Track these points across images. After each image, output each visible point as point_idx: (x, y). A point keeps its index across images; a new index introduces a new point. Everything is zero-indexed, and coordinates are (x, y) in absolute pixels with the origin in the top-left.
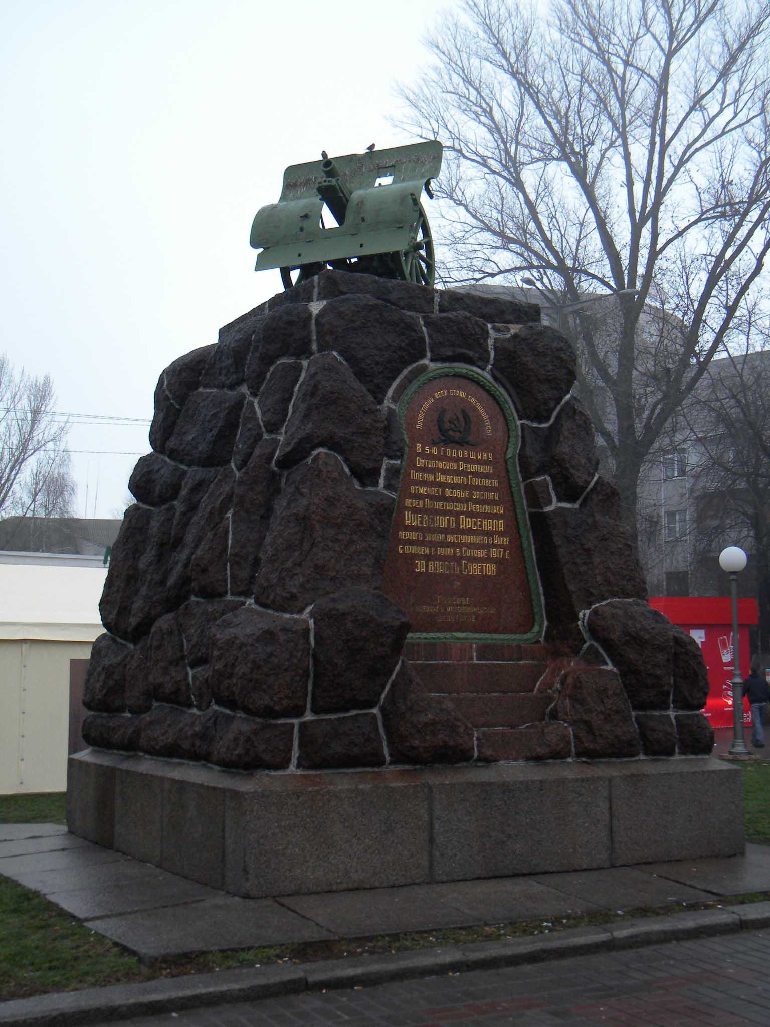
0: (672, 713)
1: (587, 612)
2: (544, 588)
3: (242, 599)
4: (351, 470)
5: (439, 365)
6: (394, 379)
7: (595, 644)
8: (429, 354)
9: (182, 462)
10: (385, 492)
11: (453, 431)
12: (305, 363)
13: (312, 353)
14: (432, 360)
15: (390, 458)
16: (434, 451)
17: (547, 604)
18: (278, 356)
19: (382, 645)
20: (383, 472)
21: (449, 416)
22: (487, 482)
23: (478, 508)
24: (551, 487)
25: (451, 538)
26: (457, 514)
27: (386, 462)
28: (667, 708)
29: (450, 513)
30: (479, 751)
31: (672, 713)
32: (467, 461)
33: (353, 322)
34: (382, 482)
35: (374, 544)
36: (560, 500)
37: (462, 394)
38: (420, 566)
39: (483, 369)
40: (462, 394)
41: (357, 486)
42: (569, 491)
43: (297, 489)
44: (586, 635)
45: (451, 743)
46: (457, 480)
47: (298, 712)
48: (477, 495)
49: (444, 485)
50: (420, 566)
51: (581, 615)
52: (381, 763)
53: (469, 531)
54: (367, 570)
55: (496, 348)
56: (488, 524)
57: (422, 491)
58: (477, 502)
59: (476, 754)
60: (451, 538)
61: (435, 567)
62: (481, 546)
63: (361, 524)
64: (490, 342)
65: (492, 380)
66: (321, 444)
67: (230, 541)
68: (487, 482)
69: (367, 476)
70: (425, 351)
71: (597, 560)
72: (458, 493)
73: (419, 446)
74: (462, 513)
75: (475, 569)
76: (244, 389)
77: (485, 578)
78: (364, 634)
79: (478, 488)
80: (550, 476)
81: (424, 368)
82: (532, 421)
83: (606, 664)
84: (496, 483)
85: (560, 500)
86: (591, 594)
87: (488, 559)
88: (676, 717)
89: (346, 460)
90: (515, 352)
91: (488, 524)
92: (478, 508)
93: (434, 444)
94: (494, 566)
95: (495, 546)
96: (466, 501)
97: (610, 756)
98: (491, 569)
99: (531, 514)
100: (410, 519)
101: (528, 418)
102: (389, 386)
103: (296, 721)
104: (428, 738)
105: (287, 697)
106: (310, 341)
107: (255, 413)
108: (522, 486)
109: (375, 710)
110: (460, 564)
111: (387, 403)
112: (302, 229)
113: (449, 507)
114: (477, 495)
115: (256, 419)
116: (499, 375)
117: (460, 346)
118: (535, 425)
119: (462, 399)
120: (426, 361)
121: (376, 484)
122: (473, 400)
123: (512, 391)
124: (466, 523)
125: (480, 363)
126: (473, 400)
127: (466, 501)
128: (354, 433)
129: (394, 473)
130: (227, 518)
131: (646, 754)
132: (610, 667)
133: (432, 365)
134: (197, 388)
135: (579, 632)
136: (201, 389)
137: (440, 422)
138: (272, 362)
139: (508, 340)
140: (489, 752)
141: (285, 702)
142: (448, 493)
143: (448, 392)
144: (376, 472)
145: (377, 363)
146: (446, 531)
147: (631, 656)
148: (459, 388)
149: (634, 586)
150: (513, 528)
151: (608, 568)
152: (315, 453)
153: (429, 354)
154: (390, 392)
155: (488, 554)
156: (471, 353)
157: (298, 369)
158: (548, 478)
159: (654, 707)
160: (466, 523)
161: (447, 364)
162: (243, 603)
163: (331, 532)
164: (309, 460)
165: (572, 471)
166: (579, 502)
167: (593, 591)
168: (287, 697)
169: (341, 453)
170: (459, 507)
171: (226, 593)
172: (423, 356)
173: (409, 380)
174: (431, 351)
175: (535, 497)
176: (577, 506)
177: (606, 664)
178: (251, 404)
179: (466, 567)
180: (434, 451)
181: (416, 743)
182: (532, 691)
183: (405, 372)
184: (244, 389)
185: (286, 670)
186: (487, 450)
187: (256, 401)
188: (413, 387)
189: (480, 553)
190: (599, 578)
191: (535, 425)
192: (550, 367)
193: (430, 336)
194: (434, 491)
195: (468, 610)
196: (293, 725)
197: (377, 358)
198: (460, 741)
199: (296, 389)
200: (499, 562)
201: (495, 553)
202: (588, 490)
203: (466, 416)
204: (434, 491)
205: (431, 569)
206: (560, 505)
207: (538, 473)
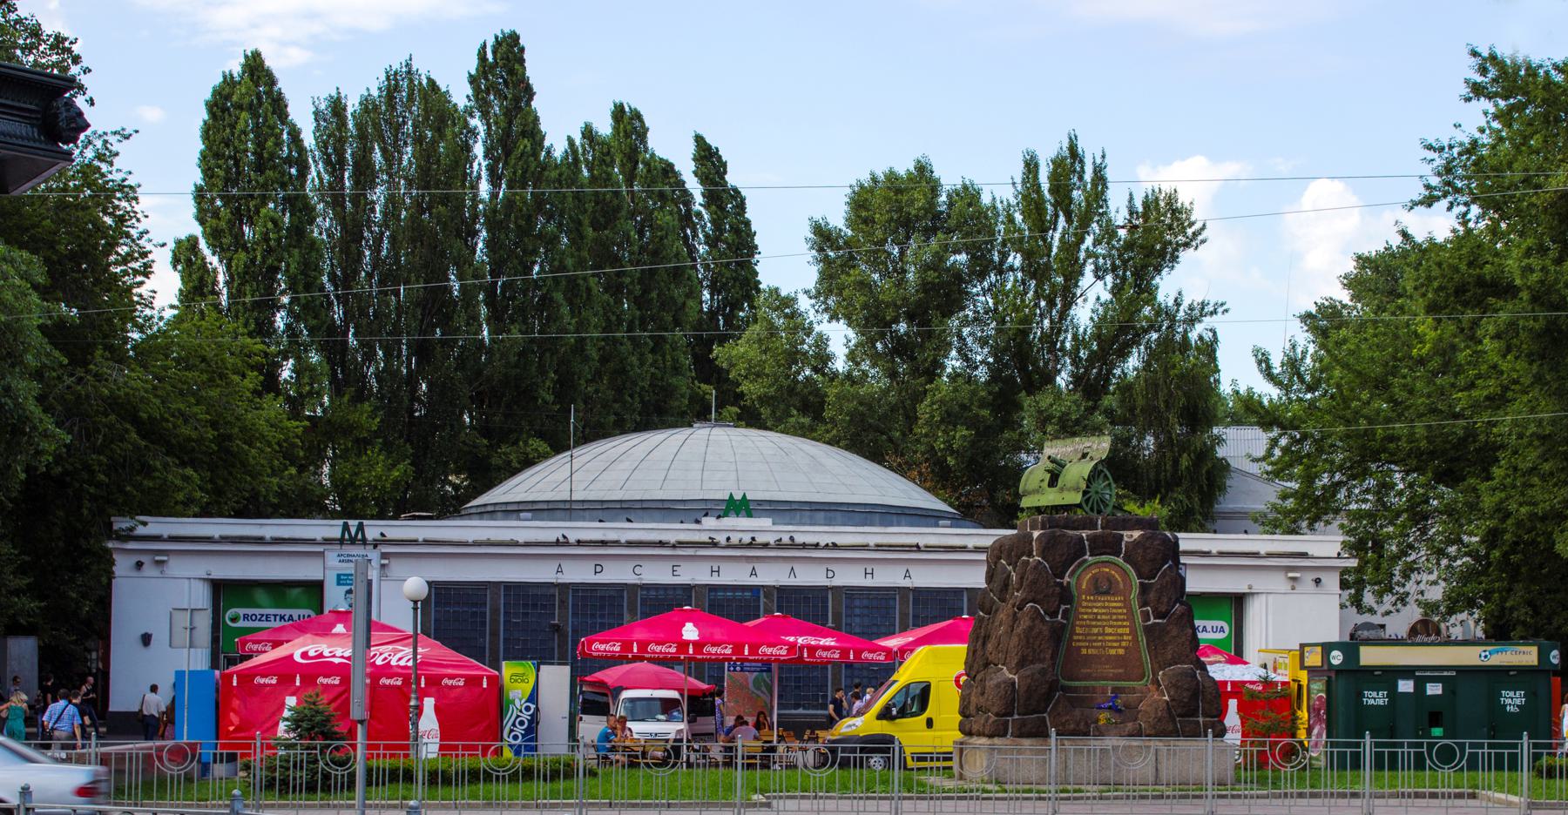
0: (1201, 720)
11: (1103, 588)
38: (1084, 651)
50: (1084, 651)
56: (1120, 631)
69: (1054, 614)
75: (1113, 652)
77: (1117, 656)
91: (1120, 631)
98: (1121, 651)
100: (1078, 630)
111: (1067, 579)
124: (1108, 630)
129: (1066, 612)
150: (1133, 632)
160: (1108, 630)
173: (1080, 565)
175: (1146, 617)
200: (1126, 648)
203: (1110, 580)
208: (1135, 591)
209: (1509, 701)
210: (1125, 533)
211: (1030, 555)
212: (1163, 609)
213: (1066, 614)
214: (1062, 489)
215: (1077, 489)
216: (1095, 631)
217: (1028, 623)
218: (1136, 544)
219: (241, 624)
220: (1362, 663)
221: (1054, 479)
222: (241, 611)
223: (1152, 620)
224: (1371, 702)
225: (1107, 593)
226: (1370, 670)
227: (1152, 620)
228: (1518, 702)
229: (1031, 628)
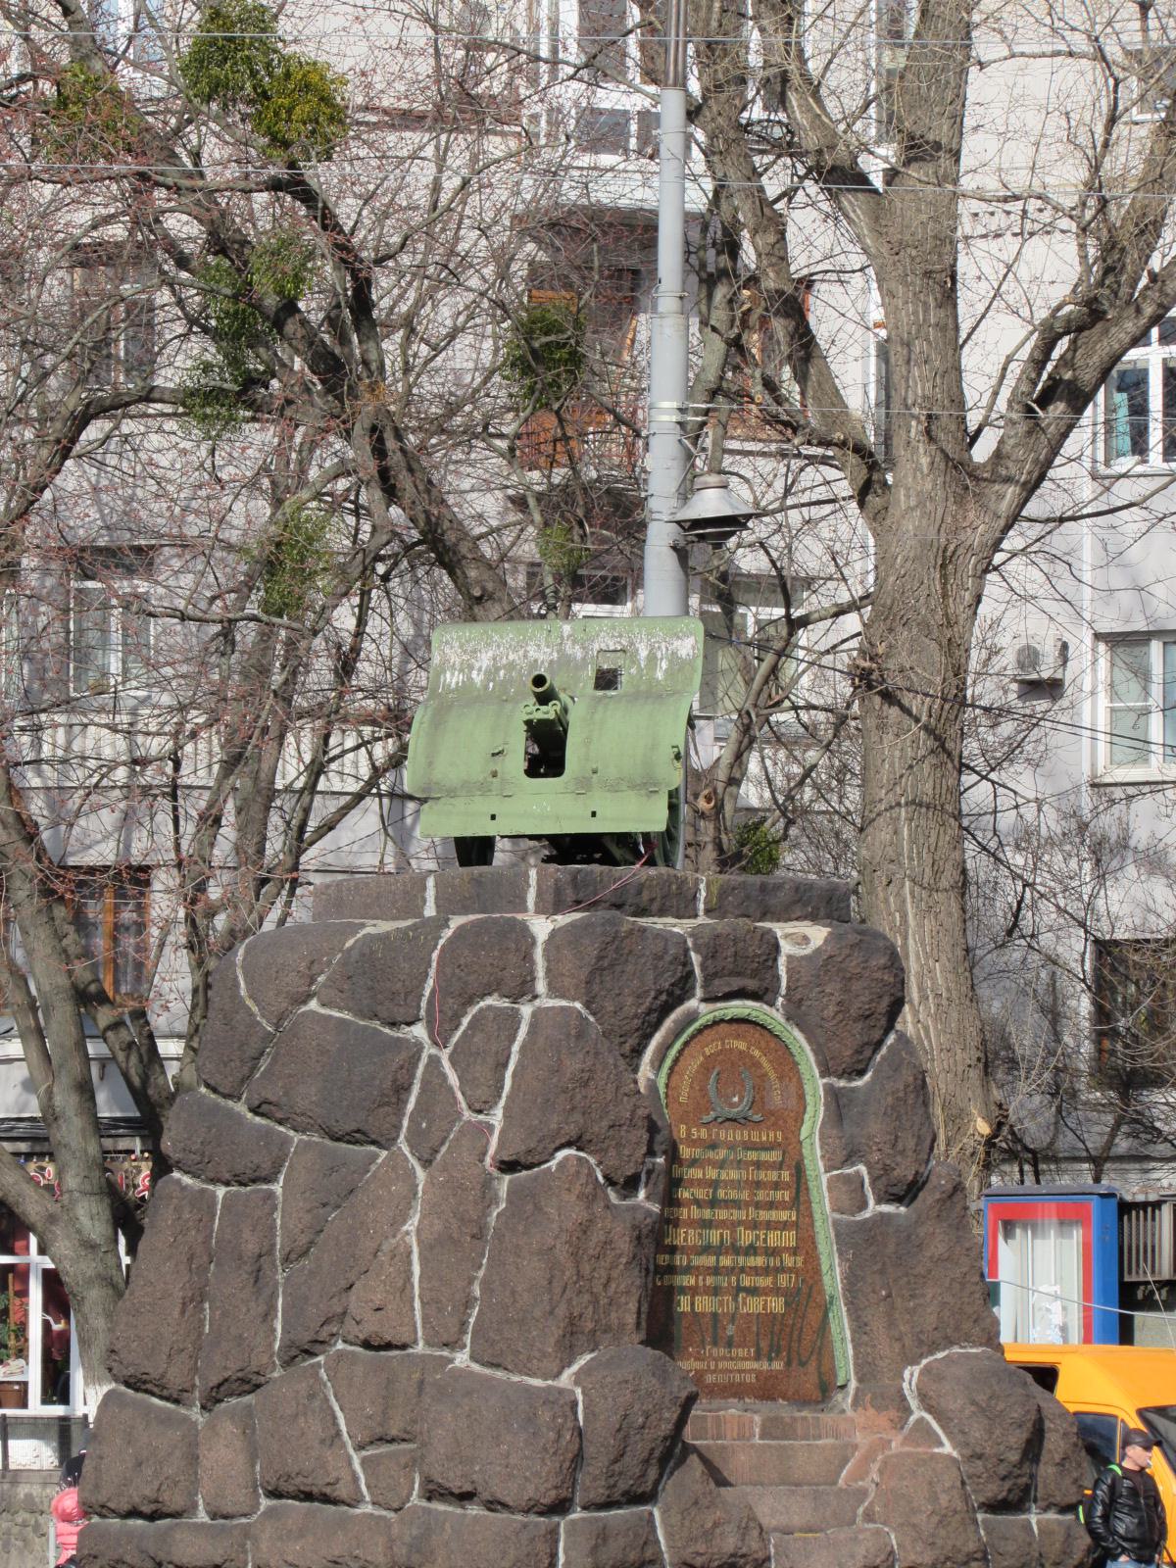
1: (917, 1369)
2: (853, 1332)
3: (445, 1353)
4: (605, 1177)
5: (711, 1006)
7: (928, 1417)
8: (699, 992)
9: (280, 1122)
12: (526, 1010)
13: (536, 997)
14: (705, 1000)
16: (704, 1133)
17: (856, 1356)
18: (483, 996)
22: (773, 1176)
23: (764, 1215)
25: (726, 1261)
26: (733, 1225)
29: (722, 1224)
32: (750, 1146)
36: (879, 1202)
37: (742, 1045)
39: (771, 1004)
40: (742, 1045)
43: (538, 1208)
44: (914, 1403)
46: (734, 1175)
48: (761, 1195)
49: (715, 1184)
51: (906, 1374)
53: (751, 1251)
56: (774, 1239)
58: (758, 1206)
60: (726, 1261)
61: (704, 1304)
62: (765, 1271)
64: (782, 961)
66: (568, 1144)
67: (416, 1269)
68: (773, 1176)
70: (693, 988)
72: (733, 1194)
73: (683, 1128)
74: (740, 1223)
75: (753, 1305)
76: (419, 1031)
79: (758, 1184)
82: (840, 1077)
83: (941, 1444)
84: (786, 1175)
85: (879, 1202)
87: (776, 1291)
91: (774, 1239)
92: (764, 1215)
94: (782, 1300)
95: (781, 1269)
96: (747, 1204)
98: (777, 1305)
99: (836, 1223)
106: (533, 979)
107: (444, 1077)
108: (825, 1178)
110: (735, 1299)
111: (645, 1071)
112: (495, 775)
113: (722, 1214)
114: (761, 1195)
115: (450, 1089)
119: (741, 1052)
120: (692, 1003)
122: (757, 1053)
124: (746, 1237)
126: (757, 1053)
127: (747, 1204)
130: (408, 1233)
132: (948, 1448)
133: (704, 1008)
134: (305, 1002)
135: (904, 1399)
136: (313, 1005)
138: (470, 1001)
139: (804, 958)
141: (553, 1493)
142: (721, 1194)
146: (718, 1251)
148: (738, 1037)
152: (561, 1155)
153: (699, 992)
155: (775, 1283)
157: (514, 1018)
158: (862, 1169)
161: (719, 1005)
162: (451, 1361)
164: (553, 1164)
170: (737, 1215)
171: (415, 1342)
174: (705, 986)
178: (434, 1061)
180: (704, 1133)
182: (835, 1483)
183: (669, 1023)
184: (419, 1031)
186: (775, 1126)
187: (444, 1056)
189: (764, 1282)
199: (516, 1048)
201: (783, 1280)
205: (698, 1309)
208: (816, 1113)
210: (779, 929)
211: (523, 989)
212: (905, 1171)
214: (584, 786)
215: (646, 786)
216: (714, 1237)
217: (577, 1213)
218: (823, 964)
221: (547, 752)
223: (873, 1208)
229: (585, 1228)
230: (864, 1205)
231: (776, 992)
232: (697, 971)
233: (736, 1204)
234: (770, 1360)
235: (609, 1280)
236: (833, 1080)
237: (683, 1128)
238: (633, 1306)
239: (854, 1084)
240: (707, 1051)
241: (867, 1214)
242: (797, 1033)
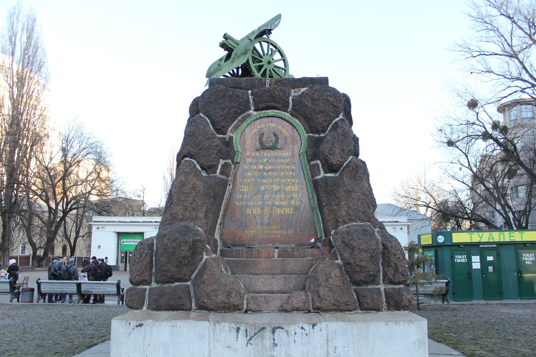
0: (382, 287)
4: (201, 167)
5: (259, 112)
6: (233, 122)
8: (252, 108)
10: (220, 176)
14: (255, 110)
15: (224, 159)
16: (257, 154)
19: (183, 250)
20: (220, 167)
21: (265, 136)
24: (320, 166)
27: (222, 162)
28: (379, 284)
30: (247, 305)
31: (382, 287)
33: (210, 99)
34: (218, 171)
35: (207, 202)
36: (325, 172)
37: (274, 125)
40: (274, 125)
41: (204, 174)
42: (330, 168)
45: (227, 301)
47: (149, 283)
52: (190, 309)
54: (202, 215)
55: (293, 100)
56: (288, 188)
57: (249, 174)
59: (245, 307)
63: (199, 192)
64: (291, 98)
65: (290, 116)
69: (210, 168)
71: (343, 203)
78: (173, 245)
80: (320, 160)
81: (250, 115)
82: (315, 133)
83: (338, 259)
85: (325, 172)
86: (338, 221)
87: (289, 206)
88: (385, 289)
89: (198, 163)
90: (301, 100)
91: (288, 188)
93: (257, 150)
97: (336, 310)
101: (312, 132)
102: (230, 126)
103: (147, 287)
104: (213, 298)
105: (137, 275)
109: (189, 283)
111: (229, 134)
116: (293, 112)
117: (271, 102)
118: (317, 135)
120: (251, 112)
121: (216, 173)
123: (302, 119)
124: (276, 188)
125: (285, 109)
128: (200, 149)
129: (225, 166)
131: (362, 310)
132: (339, 261)
133: (255, 113)
137: (261, 140)
140: (252, 306)
143: (265, 125)
144: (215, 167)
145: (221, 116)
147: (346, 255)
148: (272, 122)
149: (366, 216)
151: (349, 207)
154: (230, 129)
156: (276, 105)
158: (319, 162)
159: (367, 283)
161: (263, 112)
163: (183, 197)
165: (330, 157)
166: (340, 172)
167: (339, 220)
168: (137, 275)
169: (195, 159)
172: (249, 109)
173: (242, 121)
176: (337, 175)
177: (338, 259)
179: (275, 211)
181: (205, 300)
183: (239, 118)
185: (138, 263)
188: (245, 124)
190: (344, 213)
191: (317, 135)
192: (322, 105)
193: (253, 100)
194: (256, 174)
195: (276, 232)
196: (146, 289)
197: (221, 113)
198: (232, 300)
201: (293, 202)
202: (344, 166)
204: (256, 174)
206: (326, 175)
207: (313, 160)
209: (526, 259)
213: (225, 169)
219: (125, 243)
220: (453, 242)
222: (125, 240)
224: (459, 261)
225: (274, 148)
226: (458, 245)
227: (322, 174)
228: (531, 259)
230: (320, 174)
231: (288, 107)
232: (251, 101)
233: (272, 177)
234: (287, 230)
235: (194, 201)
236: (311, 134)
237: (248, 153)
238: (204, 210)
239: (321, 136)
240: (258, 127)
241: (319, 177)
242: (296, 120)
